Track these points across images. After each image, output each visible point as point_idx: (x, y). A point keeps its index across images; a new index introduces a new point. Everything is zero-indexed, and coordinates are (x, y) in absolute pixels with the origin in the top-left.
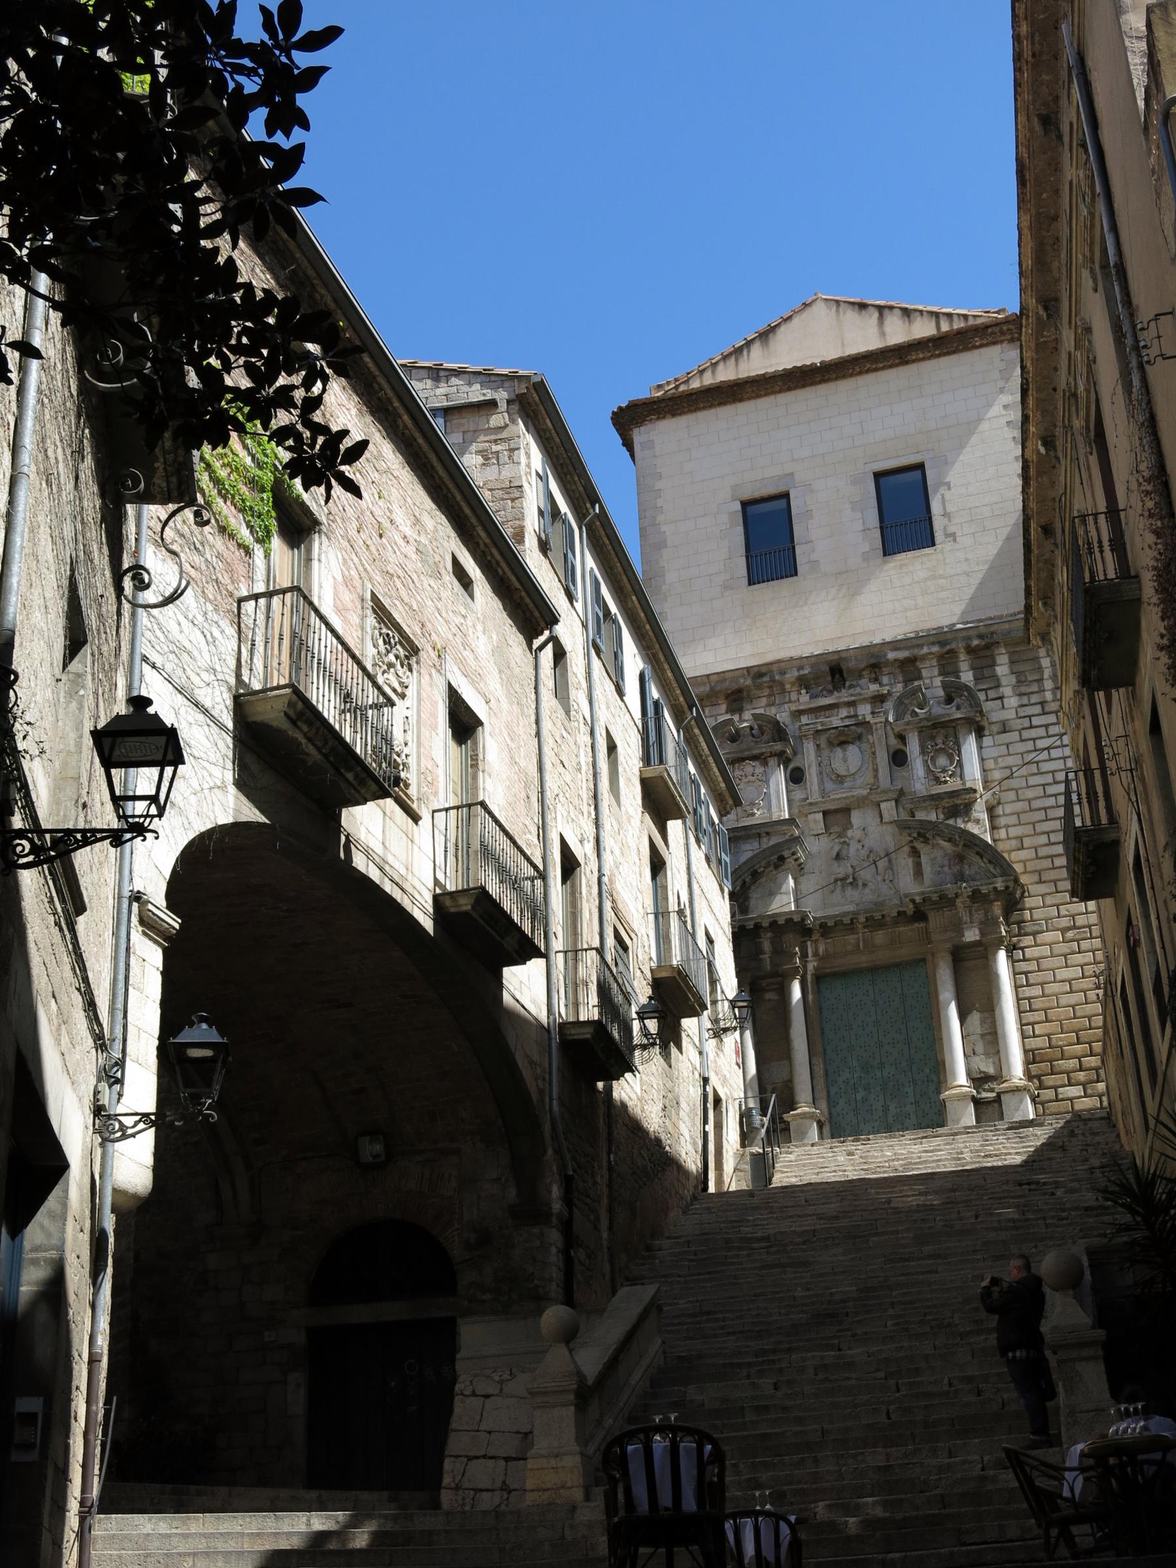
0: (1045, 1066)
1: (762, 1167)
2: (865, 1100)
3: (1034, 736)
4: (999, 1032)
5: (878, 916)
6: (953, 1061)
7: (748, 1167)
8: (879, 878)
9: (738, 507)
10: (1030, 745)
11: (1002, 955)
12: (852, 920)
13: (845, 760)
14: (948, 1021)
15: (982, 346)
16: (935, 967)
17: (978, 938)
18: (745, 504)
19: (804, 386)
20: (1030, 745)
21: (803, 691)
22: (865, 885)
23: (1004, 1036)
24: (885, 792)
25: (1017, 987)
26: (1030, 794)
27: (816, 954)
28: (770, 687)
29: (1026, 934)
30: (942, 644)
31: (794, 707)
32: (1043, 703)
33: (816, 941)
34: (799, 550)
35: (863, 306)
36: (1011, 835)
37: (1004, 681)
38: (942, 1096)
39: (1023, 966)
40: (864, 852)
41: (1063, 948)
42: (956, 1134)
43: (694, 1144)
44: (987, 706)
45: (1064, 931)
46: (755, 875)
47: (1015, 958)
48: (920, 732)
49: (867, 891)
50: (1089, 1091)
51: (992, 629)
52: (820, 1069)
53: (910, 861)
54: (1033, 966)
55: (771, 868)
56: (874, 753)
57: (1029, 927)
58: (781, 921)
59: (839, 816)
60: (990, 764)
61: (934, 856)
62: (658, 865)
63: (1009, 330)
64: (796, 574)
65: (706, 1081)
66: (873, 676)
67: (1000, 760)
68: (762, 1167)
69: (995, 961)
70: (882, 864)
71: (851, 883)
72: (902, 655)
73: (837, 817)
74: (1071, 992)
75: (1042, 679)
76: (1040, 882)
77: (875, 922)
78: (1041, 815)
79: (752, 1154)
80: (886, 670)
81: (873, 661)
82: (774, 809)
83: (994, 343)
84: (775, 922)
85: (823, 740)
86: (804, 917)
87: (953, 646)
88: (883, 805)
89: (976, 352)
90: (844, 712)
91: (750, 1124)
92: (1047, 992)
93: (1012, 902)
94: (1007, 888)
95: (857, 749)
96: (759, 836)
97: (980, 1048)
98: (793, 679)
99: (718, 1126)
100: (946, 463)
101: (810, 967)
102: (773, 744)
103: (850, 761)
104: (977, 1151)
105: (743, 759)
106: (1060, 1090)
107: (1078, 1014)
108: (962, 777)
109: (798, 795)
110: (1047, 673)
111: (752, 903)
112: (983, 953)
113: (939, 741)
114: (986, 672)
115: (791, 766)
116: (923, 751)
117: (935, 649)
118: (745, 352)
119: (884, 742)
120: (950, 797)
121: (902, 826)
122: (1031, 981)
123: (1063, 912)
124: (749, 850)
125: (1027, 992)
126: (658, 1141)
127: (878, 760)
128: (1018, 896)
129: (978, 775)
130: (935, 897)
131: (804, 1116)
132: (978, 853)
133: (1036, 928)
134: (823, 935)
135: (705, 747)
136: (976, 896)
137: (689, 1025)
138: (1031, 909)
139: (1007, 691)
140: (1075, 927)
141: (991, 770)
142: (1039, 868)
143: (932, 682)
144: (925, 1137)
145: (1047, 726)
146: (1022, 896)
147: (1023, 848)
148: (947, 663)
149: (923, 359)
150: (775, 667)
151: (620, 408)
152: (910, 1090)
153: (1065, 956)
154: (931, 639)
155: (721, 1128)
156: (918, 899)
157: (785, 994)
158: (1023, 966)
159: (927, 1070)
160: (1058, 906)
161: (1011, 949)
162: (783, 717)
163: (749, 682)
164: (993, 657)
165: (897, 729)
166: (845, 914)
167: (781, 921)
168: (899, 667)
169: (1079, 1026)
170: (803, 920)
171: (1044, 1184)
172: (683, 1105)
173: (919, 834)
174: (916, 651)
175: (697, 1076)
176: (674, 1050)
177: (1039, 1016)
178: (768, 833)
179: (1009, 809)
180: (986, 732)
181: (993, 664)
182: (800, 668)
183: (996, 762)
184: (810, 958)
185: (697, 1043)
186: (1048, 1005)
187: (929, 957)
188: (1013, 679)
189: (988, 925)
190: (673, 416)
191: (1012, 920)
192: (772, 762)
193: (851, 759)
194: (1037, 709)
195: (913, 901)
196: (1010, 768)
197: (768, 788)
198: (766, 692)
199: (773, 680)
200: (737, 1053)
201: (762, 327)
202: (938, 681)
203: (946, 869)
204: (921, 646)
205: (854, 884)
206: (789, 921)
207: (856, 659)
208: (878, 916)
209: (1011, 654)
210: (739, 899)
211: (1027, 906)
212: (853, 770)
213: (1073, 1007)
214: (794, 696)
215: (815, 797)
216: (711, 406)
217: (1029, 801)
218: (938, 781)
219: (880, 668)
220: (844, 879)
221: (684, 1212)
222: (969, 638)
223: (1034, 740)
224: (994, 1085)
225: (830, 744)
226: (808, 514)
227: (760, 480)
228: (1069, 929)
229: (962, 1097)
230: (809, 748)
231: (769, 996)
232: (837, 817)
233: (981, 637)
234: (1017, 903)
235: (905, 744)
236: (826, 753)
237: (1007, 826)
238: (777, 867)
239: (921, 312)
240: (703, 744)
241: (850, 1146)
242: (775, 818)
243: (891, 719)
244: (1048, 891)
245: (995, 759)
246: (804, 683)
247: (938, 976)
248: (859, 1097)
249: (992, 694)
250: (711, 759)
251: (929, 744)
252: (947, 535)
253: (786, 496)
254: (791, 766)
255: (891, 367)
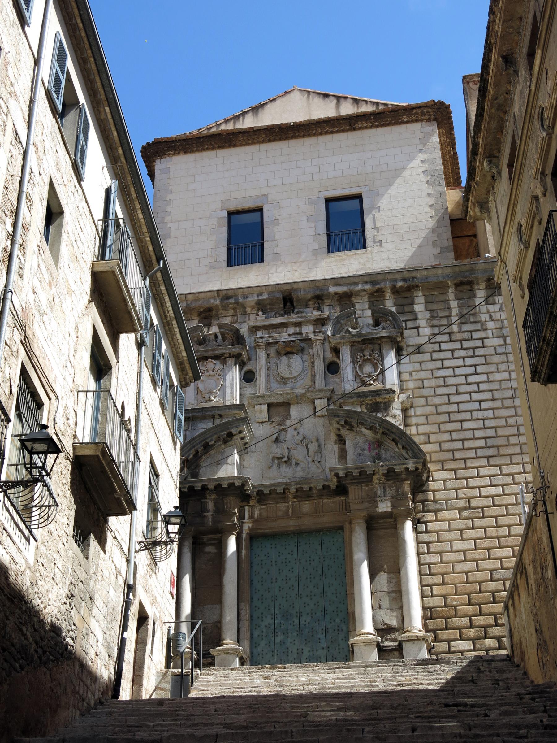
0: (440, 622)
1: (182, 683)
2: (282, 643)
3: (442, 357)
4: (403, 589)
5: (306, 488)
6: (362, 611)
7: (168, 686)
8: (310, 459)
9: (225, 214)
10: (439, 364)
11: (409, 525)
12: (284, 490)
13: (289, 366)
14: (359, 576)
15: (407, 122)
16: (351, 531)
17: (389, 509)
18: (231, 214)
19: (280, 140)
20: (439, 364)
21: (260, 313)
22: (297, 464)
23: (408, 593)
24: (320, 391)
25: (419, 554)
26: (437, 401)
27: (251, 517)
28: (235, 309)
29: (429, 511)
30: (373, 283)
31: (251, 324)
32: (450, 334)
33: (252, 506)
34: (266, 245)
35: (326, 96)
36: (420, 432)
37: (420, 316)
38: (351, 641)
39: (425, 537)
40: (300, 438)
41: (460, 524)
42: (367, 667)
43: (108, 648)
44: (407, 333)
45: (461, 510)
46: (207, 447)
47: (419, 530)
48: (351, 346)
49: (299, 469)
50: (478, 646)
51: (414, 274)
52: (246, 613)
53: (336, 447)
54: (434, 537)
55: (221, 443)
56: (313, 363)
57: (432, 506)
58: (225, 485)
59: (281, 409)
60: (406, 377)
61: (357, 442)
62: (101, 367)
63: (428, 112)
64: (263, 261)
65: (130, 588)
66: (317, 305)
67: (414, 374)
68: (182, 683)
69: (403, 529)
70: (313, 447)
71: (286, 462)
72: (341, 289)
73: (278, 408)
74: (465, 560)
75: (450, 316)
76: (443, 470)
77: (303, 493)
78: (445, 418)
79: (174, 674)
80: (327, 302)
81: (318, 293)
82: (228, 397)
83: (417, 121)
84: (220, 485)
85: (272, 351)
86: (245, 482)
87: (382, 285)
88: (317, 402)
89: (404, 126)
90: (291, 330)
91: (176, 647)
92: (444, 559)
93: (419, 482)
94: (417, 469)
95: (300, 359)
96: (213, 417)
97: (386, 603)
98: (253, 304)
99: (141, 643)
100: (378, 195)
101: (246, 527)
102: (234, 349)
103: (293, 366)
104: (389, 680)
105: (206, 358)
106: (453, 643)
107: (471, 579)
108: (383, 382)
109: (249, 390)
110: (454, 312)
111: (202, 470)
112: (393, 522)
113: (367, 353)
114: (407, 309)
115: (245, 369)
116: (353, 361)
117: (368, 287)
118: (241, 119)
119: (321, 355)
120: (373, 396)
121: (331, 415)
122: (432, 550)
123: (461, 494)
124: (204, 426)
125: (428, 558)
126: (56, 630)
127: (316, 368)
128: (424, 479)
129: (396, 381)
130: (356, 473)
131: (229, 652)
132: (393, 440)
133: (438, 506)
134: (259, 502)
135: (170, 309)
136: (390, 474)
137: (113, 521)
138: (434, 491)
139: (422, 323)
140: (470, 508)
141: (406, 381)
142: (442, 458)
143: (364, 313)
144: (338, 668)
145: (453, 351)
146: (427, 480)
147: (429, 442)
148: (376, 296)
149: (366, 128)
150: (239, 293)
151: (148, 144)
152: (322, 637)
153: (461, 531)
154: (366, 279)
155: (145, 644)
156: (341, 473)
157: (222, 546)
158: (425, 537)
159: (338, 621)
160: (456, 490)
161: (416, 522)
162: (244, 331)
163: (218, 302)
164: (412, 298)
165: (333, 342)
166: (279, 484)
167: (225, 485)
168: (339, 301)
169: (471, 590)
170: (243, 485)
171: (473, 706)
172: (99, 602)
173: (346, 422)
174: (352, 287)
175: (121, 581)
176: (93, 544)
177: (437, 579)
178: (221, 416)
179: (419, 411)
180: (404, 352)
181: (412, 303)
182: (260, 294)
183: (411, 375)
184: (247, 519)
185: (126, 551)
186: (444, 570)
187: (347, 526)
188: (428, 315)
189: (398, 499)
190: (186, 153)
191: (417, 499)
192: (230, 361)
193: (295, 365)
194: (446, 338)
195: (337, 475)
196: (422, 380)
197: (225, 380)
198: (231, 312)
199: (237, 303)
200: (172, 584)
201: (255, 104)
202: (369, 313)
203: (366, 452)
204: (356, 284)
205: (288, 462)
206: (232, 485)
207: (305, 291)
208: (306, 488)
209: (426, 296)
210: (190, 464)
211: (431, 488)
212: (295, 374)
213: (467, 573)
214: (252, 317)
215: (263, 392)
216: (213, 148)
217: (436, 406)
218: (364, 383)
219: (323, 300)
220: (279, 458)
221: (83, 715)
222: (396, 280)
223: (442, 360)
224: (396, 636)
225: (279, 354)
226: (276, 222)
227: (243, 198)
228: (465, 509)
229: (368, 643)
230: (261, 356)
231: (210, 549)
232: (278, 408)
233: (404, 280)
234: (423, 485)
235: (339, 357)
236: (274, 360)
237: (417, 425)
238: (225, 442)
239: (366, 101)
240: (169, 304)
241: (266, 672)
242: (228, 403)
243: (329, 333)
244: (449, 477)
245: (410, 373)
246: (261, 307)
247: (354, 539)
248: (278, 640)
249: (410, 324)
250: (174, 322)
251: (359, 355)
252: (375, 242)
253: (260, 210)
254: (245, 369)
255: (343, 131)
